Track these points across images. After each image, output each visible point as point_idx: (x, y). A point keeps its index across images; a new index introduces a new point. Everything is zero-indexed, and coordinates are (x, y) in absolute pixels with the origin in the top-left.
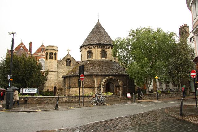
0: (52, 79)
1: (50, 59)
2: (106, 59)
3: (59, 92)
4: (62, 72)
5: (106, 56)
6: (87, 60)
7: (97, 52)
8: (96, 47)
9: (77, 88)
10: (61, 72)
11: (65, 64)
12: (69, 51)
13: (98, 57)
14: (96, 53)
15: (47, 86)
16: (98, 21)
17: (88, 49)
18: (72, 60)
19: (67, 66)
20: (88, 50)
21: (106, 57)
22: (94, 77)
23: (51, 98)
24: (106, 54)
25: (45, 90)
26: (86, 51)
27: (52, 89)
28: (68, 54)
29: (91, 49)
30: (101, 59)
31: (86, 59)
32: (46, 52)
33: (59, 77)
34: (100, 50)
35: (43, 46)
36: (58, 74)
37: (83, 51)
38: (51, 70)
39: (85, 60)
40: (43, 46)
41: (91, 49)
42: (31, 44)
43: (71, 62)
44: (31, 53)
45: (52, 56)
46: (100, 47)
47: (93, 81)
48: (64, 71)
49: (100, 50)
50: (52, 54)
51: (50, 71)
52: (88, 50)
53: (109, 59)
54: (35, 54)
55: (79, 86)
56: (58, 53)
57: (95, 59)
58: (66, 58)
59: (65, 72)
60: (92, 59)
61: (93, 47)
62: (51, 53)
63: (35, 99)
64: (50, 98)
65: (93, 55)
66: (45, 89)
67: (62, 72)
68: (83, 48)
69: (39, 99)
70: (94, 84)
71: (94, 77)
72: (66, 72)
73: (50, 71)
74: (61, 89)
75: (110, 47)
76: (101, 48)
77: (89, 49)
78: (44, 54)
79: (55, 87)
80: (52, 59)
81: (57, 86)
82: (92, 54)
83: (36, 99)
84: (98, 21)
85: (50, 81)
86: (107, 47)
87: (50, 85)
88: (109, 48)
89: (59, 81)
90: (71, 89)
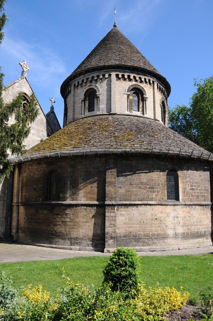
6: (127, 113)
29: (141, 85)
41: (141, 85)
60: (145, 116)
68: (113, 74)
77: (134, 83)
84: (115, 26)
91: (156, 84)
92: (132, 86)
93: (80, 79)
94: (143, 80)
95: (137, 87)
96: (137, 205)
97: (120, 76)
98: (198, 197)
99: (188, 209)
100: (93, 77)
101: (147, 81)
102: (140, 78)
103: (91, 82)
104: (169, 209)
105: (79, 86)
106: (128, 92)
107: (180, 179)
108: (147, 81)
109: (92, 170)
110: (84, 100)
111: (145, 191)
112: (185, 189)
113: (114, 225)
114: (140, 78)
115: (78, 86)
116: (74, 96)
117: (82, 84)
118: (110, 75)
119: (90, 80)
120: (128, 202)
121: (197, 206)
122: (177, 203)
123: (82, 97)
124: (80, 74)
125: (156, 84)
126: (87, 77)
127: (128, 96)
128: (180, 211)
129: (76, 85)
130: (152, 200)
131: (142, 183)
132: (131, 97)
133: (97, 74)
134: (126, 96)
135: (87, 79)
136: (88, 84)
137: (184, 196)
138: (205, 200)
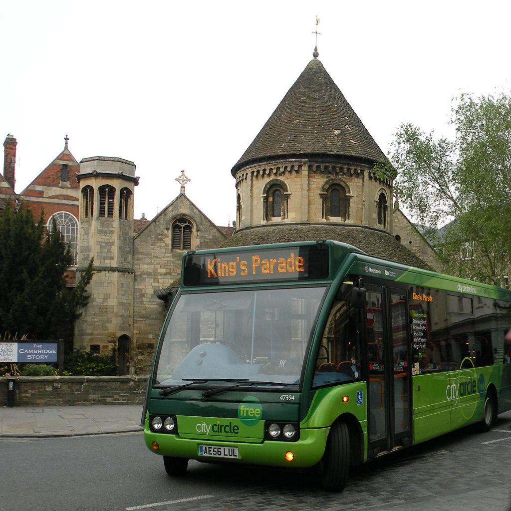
0: (113, 302)
1: (102, 213)
2: (347, 222)
3: (140, 357)
4: (154, 275)
5: (347, 206)
6: (263, 222)
7: (309, 190)
8: (305, 170)
10: (149, 274)
11: (169, 240)
12: (183, 179)
13: (313, 211)
14: (305, 192)
15: (89, 331)
17: (269, 175)
18: (198, 220)
19: (175, 245)
20: (267, 180)
21: (345, 214)
23: (118, 384)
24: (347, 199)
25: (83, 344)
26: (261, 184)
27: (111, 346)
28: (182, 196)
29: (281, 178)
30: (324, 221)
31: (259, 219)
32: (83, 184)
33: (142, 295)
34: (319, 182)
35: (66, 155)
36: (135, 280)
37: (246, 185)
38: (108, 263)
39: (254, 224)
40: (66, 155)
41: (281, 178)
42: (10, 144)
43: (194, 230)
44: (13, 186)
45: (111, 205)
46: (322, 168)
48: (163, 271)
49: (319, 182)
50: (111, 196)
51: (100, 270)
52: (267, 180)
53: (359, 223)
54: (28, 191)
56: (138, 192)
57: (299, 221)
58: (170, 215)
59: (165, 274)
60: (286, 221)
61: (293, 167)
62: (106, 192)
63: (49, 388)
64: (114, 385)
65: (292, 203)
66: (82, 347)
67: (154, 275)
68: (249, 171)
69: (65, 387)
72: (170, 274)
73: (100, 270)
75: (362, 171)
76: (326, 171)
77: (272, 177)
78: (79, 194)
79: (124, 339)
80: (111, 213)
81: (135, 335)
82: (287, 197)
83: (55, 388)
85: (104, 310)
86: (349, 170)
87: (104, 327)
88: (357, 175)
89: (144, 312)
94: (282, 170)
95: (275, 182)
101: (289, 169)
106: (264, 194)
108: (289, 169)
114: (278, 168)
118: (247, 174)
127: (264, 200)
132: (271, 199)
134: (262, 200)
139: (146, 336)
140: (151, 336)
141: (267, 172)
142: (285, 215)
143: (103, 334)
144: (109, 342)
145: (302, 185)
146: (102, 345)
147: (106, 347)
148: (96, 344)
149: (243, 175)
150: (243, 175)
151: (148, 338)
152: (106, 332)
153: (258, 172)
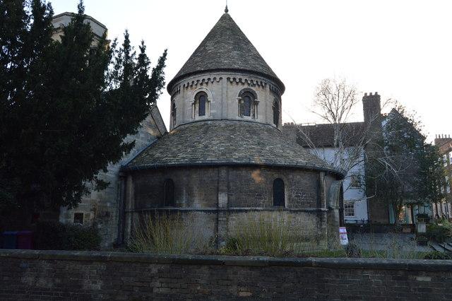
6: (238, 118)
9: (266, 213)
16: (226, 11)
17: (243, 84)
20: (240, 88)
22: (322, 174)
39: (230, 118)
41: (253, 88)
47: (319, 186)
55: (278, 201)
57: (264, 122)
60: (256, 120)
65: (261, 107)
66: (67, 216)
68: (224, 78)
70: (320, 204)
71: (322, 174)
74: (107, 214)
82: (256, 103)
84: (226, 11)
90: (234, 216)
91: (268, 86)
92: (243, 90)
93: (190, 80)
94: (255, 83)
96: (246, 211)
97: (232, 80)
98: (303, 203)
99: (293, 215)
100: (204, 80)
101: (259, 83)
102: (252, 81)
103: (201, 84)
104: (275, 215)
105: (189, 88)
107: (286, 187)
108: (259, 83)
109: (206, 179)
110: (195, 104)
111: (253, 198)
112: (290, 196)
113: (228, 230)
115: (187, 87)
116: (183, 97)
117: (192, 86)
118: (221, 78)
119: (201, 82)
120: (238, 208)
121: (302, 213)
122: (282, 207)
123: (193, 100)
124: (189, 75)
125: (268, 86)
126: (197, 79)
128: (286, 215)
129: (186, 86)
130: (259, 206)
131: (250, 191)
133: (208, 77)
135: (198, 81)
136: (199, 86)
137: (290, 202)
138: (310, 207)
139: (105, 205)
140: (108, 204)
141: (243, 81)
142: (254, 115)
143: (87, 201)
144: (91, 210)
145: (266, 97)
146: (85, 213)
147: (88, 215)
148: (80, 212)
149: (215, 79)
150: (215, 79)
151: (106, 207)
152: (89, 199)
153: (234, 79)
